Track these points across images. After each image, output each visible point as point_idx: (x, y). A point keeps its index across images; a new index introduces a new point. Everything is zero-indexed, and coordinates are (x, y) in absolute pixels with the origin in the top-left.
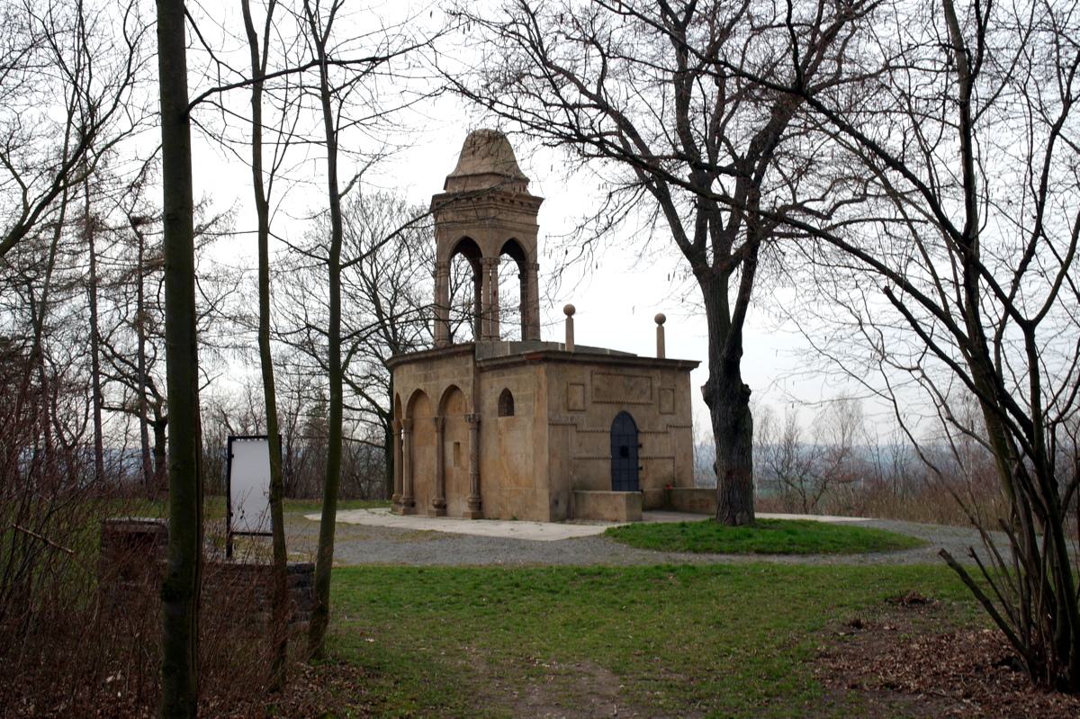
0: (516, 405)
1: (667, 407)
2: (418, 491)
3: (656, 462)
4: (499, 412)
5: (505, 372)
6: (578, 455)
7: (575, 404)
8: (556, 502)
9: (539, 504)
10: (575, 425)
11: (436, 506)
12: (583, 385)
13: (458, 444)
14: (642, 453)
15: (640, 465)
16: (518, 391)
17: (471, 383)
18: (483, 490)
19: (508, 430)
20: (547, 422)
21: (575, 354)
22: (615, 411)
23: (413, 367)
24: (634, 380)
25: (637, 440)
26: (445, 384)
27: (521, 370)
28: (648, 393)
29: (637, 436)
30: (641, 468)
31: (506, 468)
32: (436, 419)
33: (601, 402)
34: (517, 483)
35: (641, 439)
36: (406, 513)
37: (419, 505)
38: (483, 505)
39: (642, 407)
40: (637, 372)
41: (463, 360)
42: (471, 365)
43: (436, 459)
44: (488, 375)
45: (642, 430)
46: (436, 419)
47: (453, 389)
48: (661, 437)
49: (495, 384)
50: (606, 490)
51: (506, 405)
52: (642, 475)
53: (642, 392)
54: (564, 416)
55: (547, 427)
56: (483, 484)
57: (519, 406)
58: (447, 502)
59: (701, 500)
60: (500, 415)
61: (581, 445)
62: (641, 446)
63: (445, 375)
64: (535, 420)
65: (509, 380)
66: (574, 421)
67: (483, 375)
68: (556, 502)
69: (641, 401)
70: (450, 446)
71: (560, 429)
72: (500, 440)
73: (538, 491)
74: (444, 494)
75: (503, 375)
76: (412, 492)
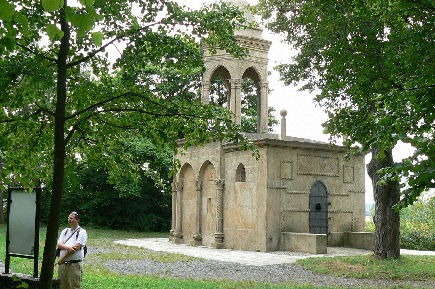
0: (246, 175)
1: (349, 179)
2: (185, 228)
3: (340, 215)
4: (236, 179)
6: (286, 209)
7: (285, 175)
8: (271, 239)
9: (259, 241)
10: (286, 189)
11: (195, 239)
12: (292, 162)
13: (210, 199)
14: (330, 209)
15: (329, 217)
16: (248, 165)
17: (219, 159)
18: (225, 229)
20: (266, 186)
21: (286, 142)
22: (313, 180)
24: (326, 160)
25: (327, 200)
26: (203, 160)
28: (336, 169)
29: (327, 197)
30: (330, 218)
31: (239, 215)
32: (197, 183)
33: (304, 174)
34: (246, 226)
35: (330, 199)
36: (177, 242)
37: (185, 237)
38: (225, 239)
39: (331, 178)
40: (329, 154)
42: (219, 148)
43: (196, 208)
44: (230, 154)
45: (330, 193)
46: (197, 183)
47: (208, 164)
48: (344, 198)
49: (234, 161)
50: (305, 232)
51: (241, 175)
52: (330, 223)
53: (332, 168)
54: (278, 183)
55: (266, 189)
56: (225, 225)
58: (203, 237)
59: (368, 241)
60: (236, 182)
61: (289, 202)
62: (330, 204)
63: (203, 154)
64: (258, 185)
66: (284, 187)
67: (227, 155)
68: (271, 239)
69: (331, 174)
70: (205, 200)
71: (274, 191)
73: (259, 232)
74: (200, 231)
75: (240, 155)
76: (181, 229)
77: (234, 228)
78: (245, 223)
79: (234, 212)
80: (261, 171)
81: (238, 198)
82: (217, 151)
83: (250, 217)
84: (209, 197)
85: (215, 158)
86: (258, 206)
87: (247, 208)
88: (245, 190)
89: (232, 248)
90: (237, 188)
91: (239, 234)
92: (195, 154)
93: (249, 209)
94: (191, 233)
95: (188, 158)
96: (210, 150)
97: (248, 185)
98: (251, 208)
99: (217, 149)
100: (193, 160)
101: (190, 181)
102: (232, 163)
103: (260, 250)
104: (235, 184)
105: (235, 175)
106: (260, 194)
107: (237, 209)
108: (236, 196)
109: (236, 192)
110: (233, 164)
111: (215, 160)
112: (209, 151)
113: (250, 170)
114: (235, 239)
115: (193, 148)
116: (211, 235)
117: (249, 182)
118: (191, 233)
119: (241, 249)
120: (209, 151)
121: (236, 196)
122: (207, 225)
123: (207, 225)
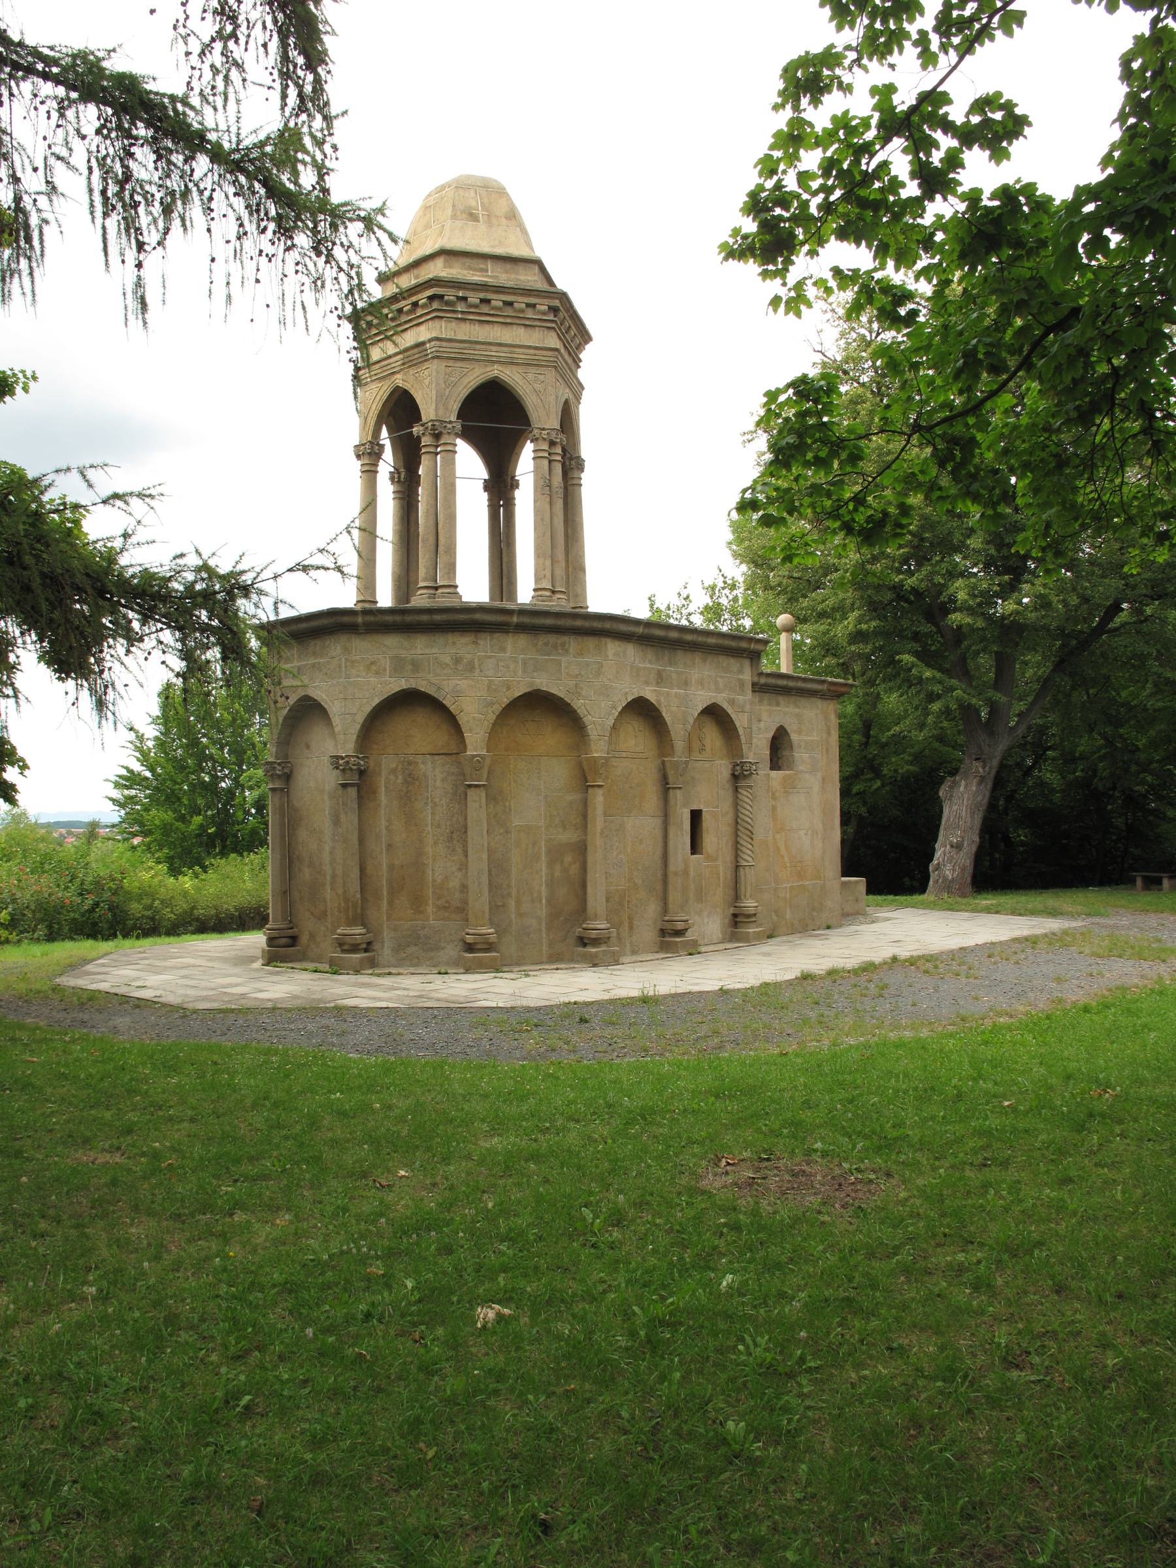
5: (781, 699)
31: (783, 851)
41: (734, 664)
42: (747, 676)
49: (765, 717)
57: (801, 756)
60: (772, 769)
63: (701, 683)
64: (824, 779)
72: (774, 808)
75: (778, 705)
80: (827, 750)
82: (742, 684)
84: (695, 808)
87: (802, 833)
89: (768, 933)
92: (674, 676)
95: (647, 683)
96: (722, 677)
100: (668, 694)
101: (624, 755)
102: (760, 721)
103: (830, 922)
105: (768, 752)
107: (778, 836)
109: (773, 794)
110: (762, 725)
113: (803, 744)
114: (776, 912)
115: (666, 658)
116: (705, 913)
118: (631, 919)
122: (692, 886)
123: (692, 886)
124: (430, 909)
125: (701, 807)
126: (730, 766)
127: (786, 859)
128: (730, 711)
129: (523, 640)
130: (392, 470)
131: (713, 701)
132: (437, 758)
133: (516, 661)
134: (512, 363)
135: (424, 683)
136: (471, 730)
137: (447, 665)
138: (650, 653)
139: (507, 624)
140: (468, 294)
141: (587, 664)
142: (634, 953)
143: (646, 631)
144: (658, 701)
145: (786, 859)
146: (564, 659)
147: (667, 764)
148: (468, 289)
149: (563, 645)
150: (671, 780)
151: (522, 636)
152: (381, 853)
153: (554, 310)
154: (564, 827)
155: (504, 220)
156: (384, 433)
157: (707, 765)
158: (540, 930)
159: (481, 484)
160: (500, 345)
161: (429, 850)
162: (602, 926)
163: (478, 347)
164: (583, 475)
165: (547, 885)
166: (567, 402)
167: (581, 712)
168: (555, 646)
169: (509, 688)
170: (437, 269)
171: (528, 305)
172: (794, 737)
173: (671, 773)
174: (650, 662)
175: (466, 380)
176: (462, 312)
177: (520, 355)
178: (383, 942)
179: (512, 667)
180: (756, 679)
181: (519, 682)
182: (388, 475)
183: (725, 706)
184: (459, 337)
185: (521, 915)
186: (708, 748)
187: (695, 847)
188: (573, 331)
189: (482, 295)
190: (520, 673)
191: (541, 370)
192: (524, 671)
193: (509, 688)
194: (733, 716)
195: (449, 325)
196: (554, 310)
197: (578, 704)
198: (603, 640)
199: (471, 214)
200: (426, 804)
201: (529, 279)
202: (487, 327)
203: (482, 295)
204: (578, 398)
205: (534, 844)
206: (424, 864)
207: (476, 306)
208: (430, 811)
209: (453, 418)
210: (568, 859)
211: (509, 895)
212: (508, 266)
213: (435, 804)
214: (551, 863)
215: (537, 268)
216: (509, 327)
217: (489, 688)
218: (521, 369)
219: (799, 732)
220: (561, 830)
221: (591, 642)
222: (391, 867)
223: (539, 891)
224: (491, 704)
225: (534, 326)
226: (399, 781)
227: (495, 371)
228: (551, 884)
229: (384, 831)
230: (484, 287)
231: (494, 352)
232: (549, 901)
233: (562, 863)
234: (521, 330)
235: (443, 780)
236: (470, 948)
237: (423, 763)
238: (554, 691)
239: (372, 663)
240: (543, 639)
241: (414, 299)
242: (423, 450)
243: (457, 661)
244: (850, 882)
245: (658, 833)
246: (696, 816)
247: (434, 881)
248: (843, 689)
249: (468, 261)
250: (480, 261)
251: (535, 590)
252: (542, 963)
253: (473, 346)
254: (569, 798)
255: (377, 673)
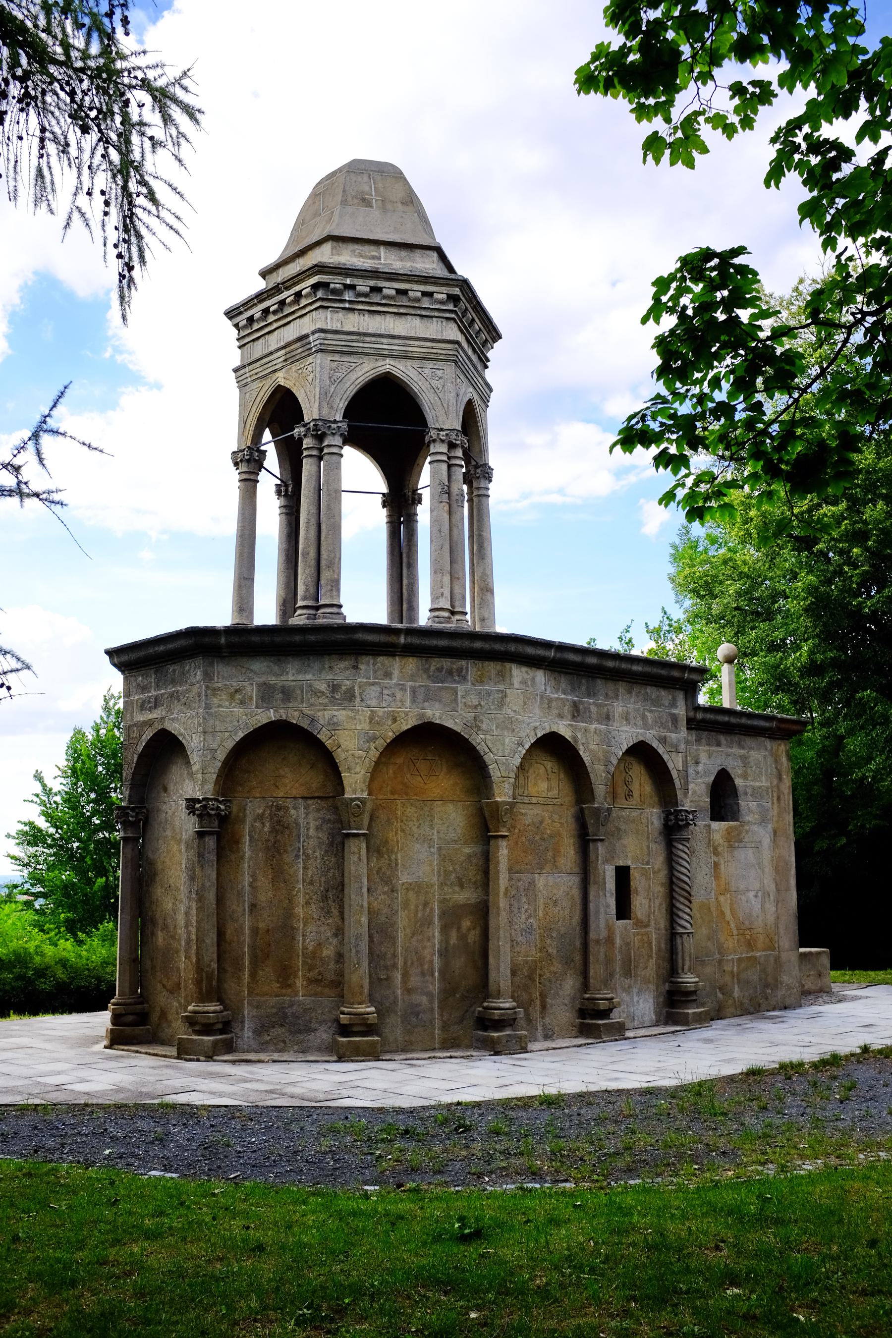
19: (731, 847)
23: (540, 676)
27: (749, 741)
34: (750, 945)
49: (703, 757)
57: (748, 805)
60: (713, 819)
63: (626, 718)
64: (775, 832)
65: (728, 755)
72: (716, 865)
73: (785, 956)
75: (719, 744)
77: (717, 956)
78: (748, 937)
79: (713, 909)
80: (779, 799)
81: (722, 867)
83: (760, 920)
84: (621, 863)
85: (668, 739)
86: (778, 890)
87: (751, 894)
88: (742, 845)
90: (718, 838)
91: (732, 972)
92: (593, 709)
93: (756, 896)
94: (543, 996)
95: (561, 716)
96: (651, 711)
97: (747, 832)
98: (760, 894)
99: (673, 711)
101: (534, 800)
103: (788, 1002)
104: (709, 826)
105: (708, 800)
106: (779, 857)
108: (715, 862)
109: (715, 849)
110: (700, 768)
111: (672, 745)
112: (648, 714)
113: (749, 791)
114: (720, 989)
115: (584, 688)
116: (635, 990)
117: (749, 823)
118: (543, 996)
119: (739, 1013)
120: (648, 714)
121: (715, 862)
122: (619, 957)
124: (300, 983)
125: (629, 863)
126: (663, 815)
127: (733, 925)
128: (661, 750)
129: (411, 664)
130: (279, 482)
131: (641, 738)
132: (310, 802)
133: (403, 688)
134: (405, 356)
135: (296, 714)
136: (349, 769)
137: (323, 693)
138: (564, 682)
139: (394, 645)
140: (356, 281)
141: (489, 694)
142: (547, 1037)
143: (559, 655)
144: (575, 738)
145: (733, 925)
146: (461, 688)
147: (586, 812)
148: (357, 276)
149: (459, 671)
150: (591, 830)
151: (411, 659)
152: (244, 914)
153: (452, 298)
154: (462, 886)
155: (400, 205)
156: (267, 435)
157: (635, 814)
158: (432, 1010)
159: (379, 499)
160: (393, 337)
161: (299, 911)
162: (507, 1005)
163: (368, 339)
164: (490, 486)
165: (440, 955)
166: (470, 403)
167: (481, 748)
168: (450, 672)
169: (395, 720)
170: (325, 255)
171: (425, 294)
172: (739, 782)
173: (590, 822)
174: (564, 693)
175: (353, 376)
176: (350, 302)
177: (415, 348)
178: (243, 1022)
179: (399, 695)
180: (691, 714)
181: (406, 714)
182: (274, 488)
183: (655, 744)
184: (346, 329)
185: (409, 991)
186: (636, 794)
187: (623, 910)
188: (478, 325)
189: (372, 283)
190: (408, 703)
191: (440, 365)
192: (414, 701)
193: (395, 720)
194: (665, 757)
195: (336, 316)
196: (452, 298)
197: (477, 740)
198: (508, 665)
199: (363, 200)
200: (297, 856)
201: (428, 265)
202: (378, 318)
203: (372, 283)
204: (486, 401)
205: (426, 904)
206: (293, 928)
207: (366, 295)
208: (301, 865)
209: (339, 417)
210: (466, 923)
211: (395, 966)
212: (404, 253)
213: (307, 856)
214: (445, 929)
215: (435, 255)
216: (403, 318)
217: (371, 719)
218: (416, 364)
219: (745, 776)
220: (457, 889)
221: (492, 667)
222: (255, 931)
223: (431, 962)
224: (374, 739)
225: (432, 317)
226: (267, 829)
227: (387, 366)
228: (444, 953)
229: (247, 888)
230: (375, 274)
231: (385, 345)
232: (444, 972)
233: (459, 928)
234: (417, 321)
235: (317, 828)
236: (345, 1030)
237: (295, 808)
238: (449, 724)
239: (236, 691)
240: (436, 663)
241: (297, 288)
242: (305, 453)
243: (335, 688)
244: (810, 953)
245: (576, 893)
246: (623, 874)
247: (305, 948)
248: (795, 727)
249: (358, 248)
250: (372, 248)
251: (431, 610)
252: (434, 1049)
253: (362, 338)
254: (467, 850)
255: (242, 702)
